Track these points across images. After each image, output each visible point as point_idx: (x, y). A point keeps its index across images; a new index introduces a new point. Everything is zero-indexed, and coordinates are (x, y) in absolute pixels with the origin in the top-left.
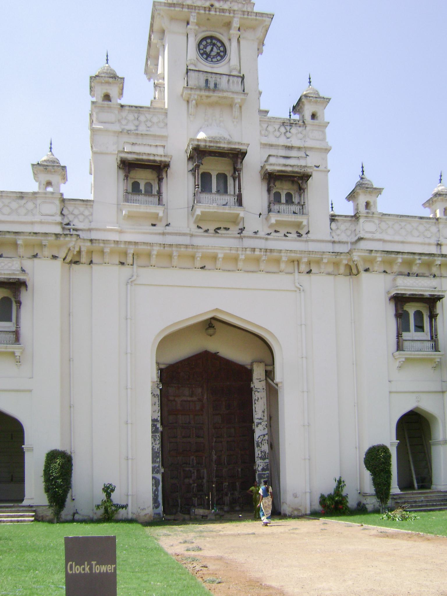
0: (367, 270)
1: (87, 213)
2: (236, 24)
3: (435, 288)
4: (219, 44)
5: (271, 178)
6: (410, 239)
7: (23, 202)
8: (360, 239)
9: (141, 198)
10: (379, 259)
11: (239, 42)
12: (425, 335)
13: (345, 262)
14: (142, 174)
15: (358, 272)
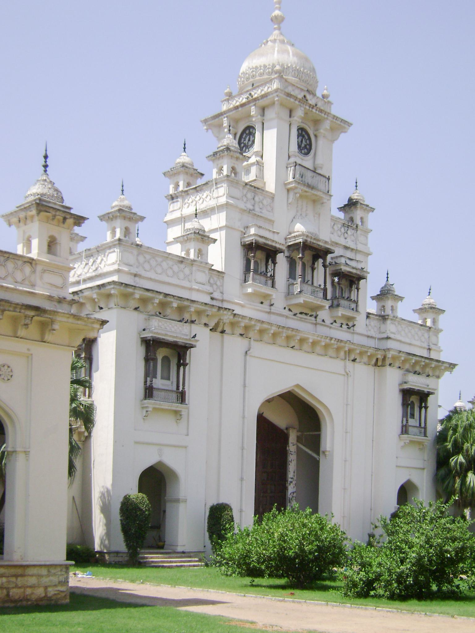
6: (414, 342)
7: (182, 266)
8: (388, 338)
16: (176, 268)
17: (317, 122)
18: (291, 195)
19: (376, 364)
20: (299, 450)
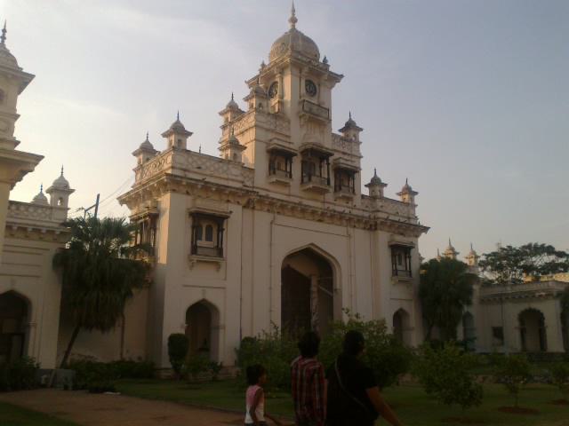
1: (251, 176)
7: (221, 164)
16: (216, 166)
17: (319, 75)
18: (302, 120)
19: (370, 229)
20: (319, 290)
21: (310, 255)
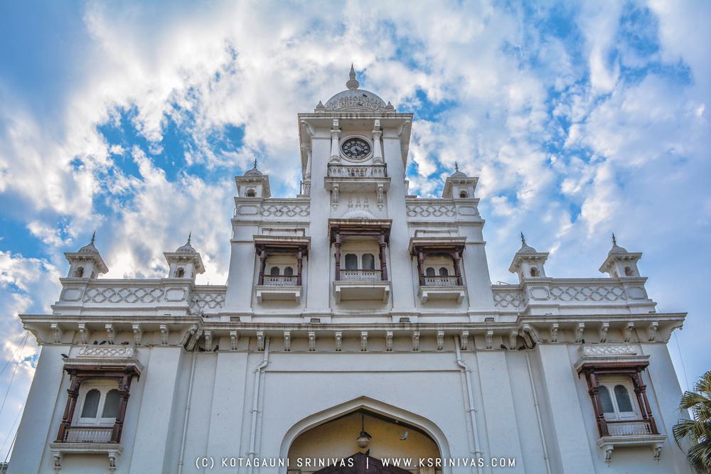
0: (545, 342)
1: (219, 299)
2: (377, 123)
3: (635, 354)
4: (363, 144)
5: (419, 251)
9: (281, 280)
10: (556, 326)
11: (381, 140)
12: (635, 414)
13: (515, 333)
14: (278, 257)
15: (534, 344)
21: (363, 418)
